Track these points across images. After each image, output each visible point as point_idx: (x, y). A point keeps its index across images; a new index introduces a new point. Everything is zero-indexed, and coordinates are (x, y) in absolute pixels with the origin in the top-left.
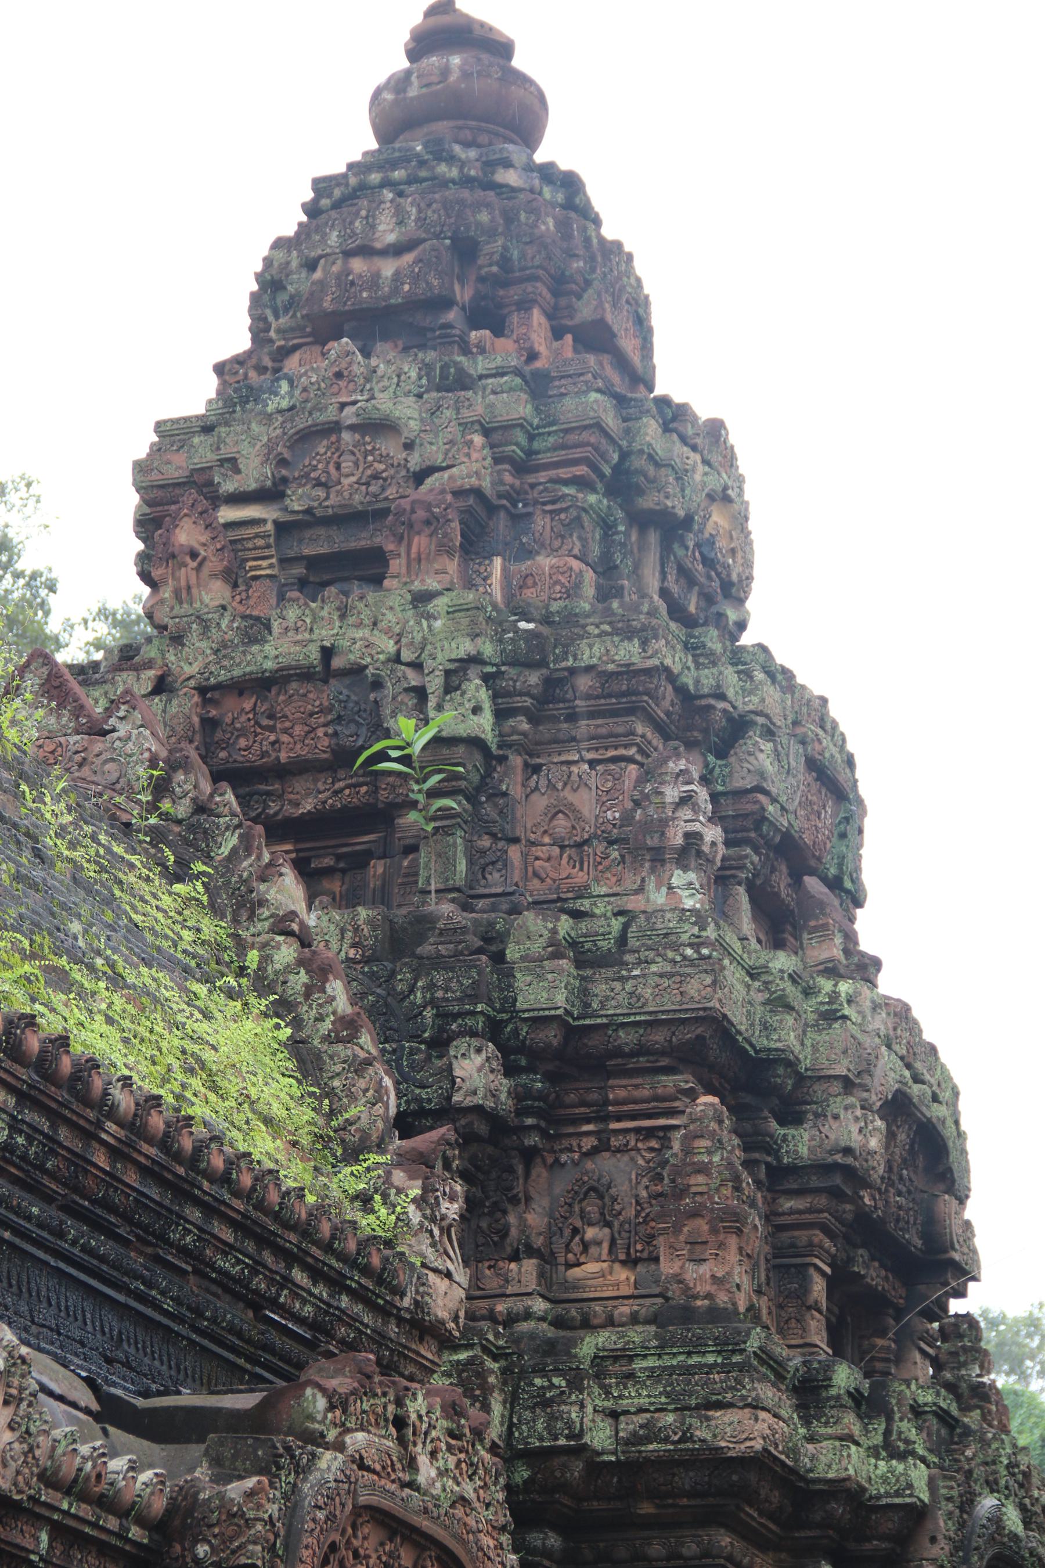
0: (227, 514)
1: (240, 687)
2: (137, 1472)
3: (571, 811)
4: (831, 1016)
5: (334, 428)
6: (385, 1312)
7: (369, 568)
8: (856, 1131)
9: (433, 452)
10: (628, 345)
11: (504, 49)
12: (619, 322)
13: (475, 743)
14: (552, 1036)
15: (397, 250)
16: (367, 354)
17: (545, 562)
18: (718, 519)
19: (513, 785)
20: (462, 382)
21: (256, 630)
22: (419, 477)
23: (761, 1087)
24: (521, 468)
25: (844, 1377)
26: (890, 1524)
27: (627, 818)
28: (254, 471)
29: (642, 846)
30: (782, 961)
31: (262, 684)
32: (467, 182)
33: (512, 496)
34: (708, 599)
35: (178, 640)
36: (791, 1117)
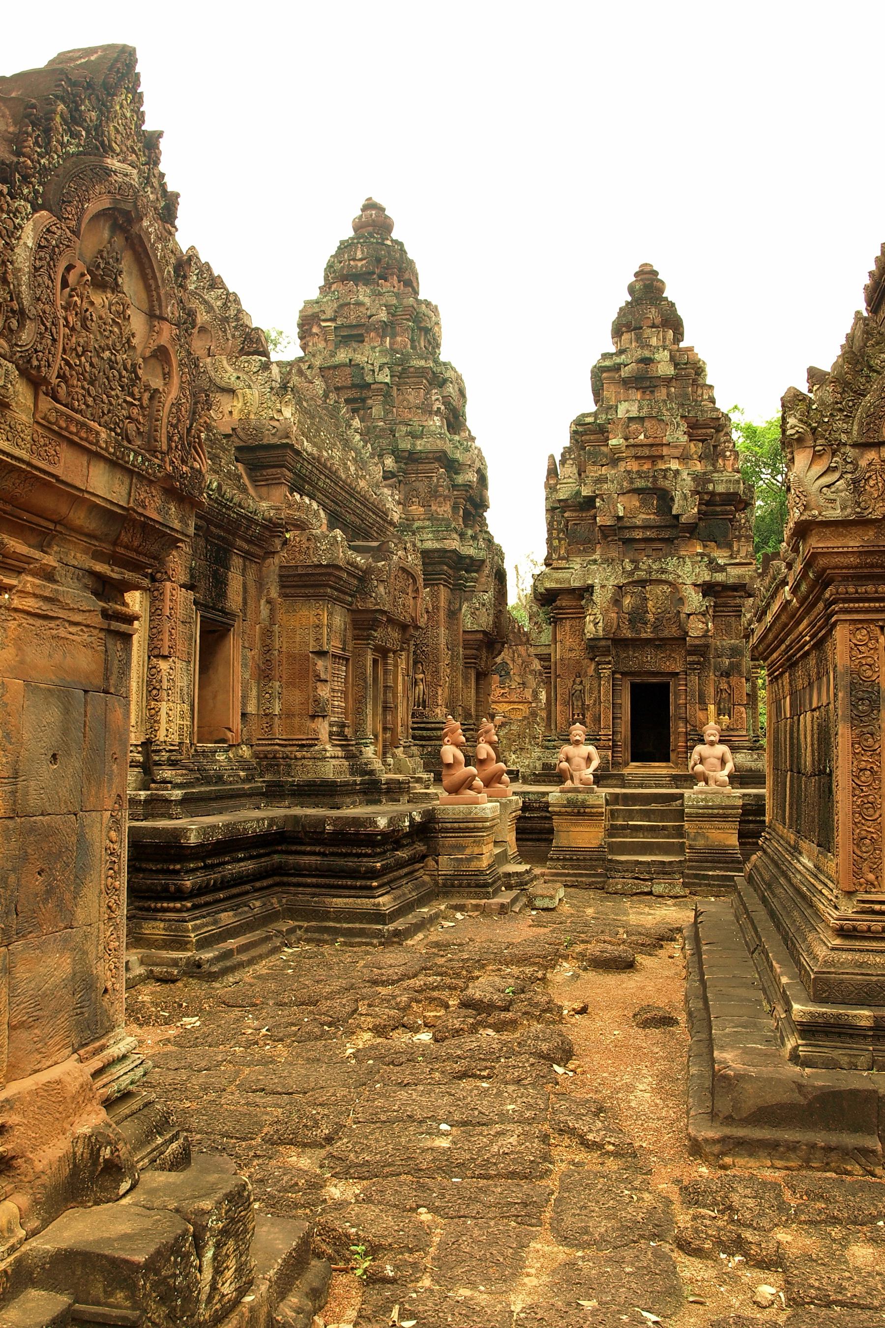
0: (323, 324)
1: (329, 368)
2: (360, 560)
3: (408, 401)
4: (467, 449)
5: (349, 304)
6: (385, 520)
7: (360, 339)
8: (473, 477)
9: (374, 311)
10: (415, 285)
11: (383, 210)
12: (414, 280)
13: (387, 383)
14: (406, 454)
15: (361, 260)
16: (357, 285)
17: (399, 339)
18: (436, 329)
19: (395, 392)
20: (380, 294)
21: (333, 355)
22: (370, 317)
23: (452, 466)
24: (393, 315)
25: (470, 532)
26: (478, 563)
27: (423, 403)
28: (329, 314)
29: (428, 411)
30: (457, 438)
31: (335, 367)
32: (377, 243)
33: (392, 323)
34: (433, 348)
35: (314, 356)
36: (457, 473)
